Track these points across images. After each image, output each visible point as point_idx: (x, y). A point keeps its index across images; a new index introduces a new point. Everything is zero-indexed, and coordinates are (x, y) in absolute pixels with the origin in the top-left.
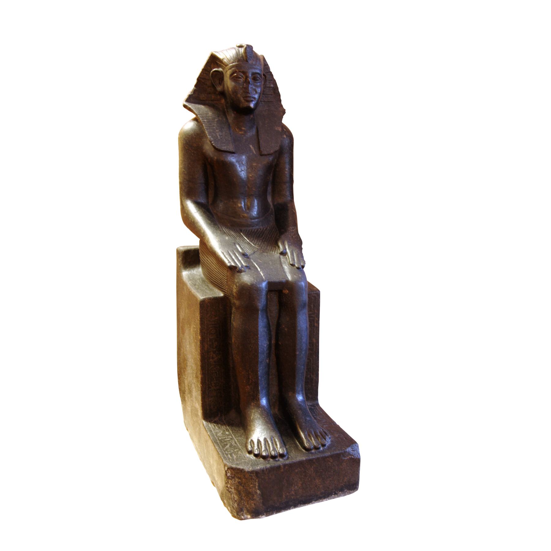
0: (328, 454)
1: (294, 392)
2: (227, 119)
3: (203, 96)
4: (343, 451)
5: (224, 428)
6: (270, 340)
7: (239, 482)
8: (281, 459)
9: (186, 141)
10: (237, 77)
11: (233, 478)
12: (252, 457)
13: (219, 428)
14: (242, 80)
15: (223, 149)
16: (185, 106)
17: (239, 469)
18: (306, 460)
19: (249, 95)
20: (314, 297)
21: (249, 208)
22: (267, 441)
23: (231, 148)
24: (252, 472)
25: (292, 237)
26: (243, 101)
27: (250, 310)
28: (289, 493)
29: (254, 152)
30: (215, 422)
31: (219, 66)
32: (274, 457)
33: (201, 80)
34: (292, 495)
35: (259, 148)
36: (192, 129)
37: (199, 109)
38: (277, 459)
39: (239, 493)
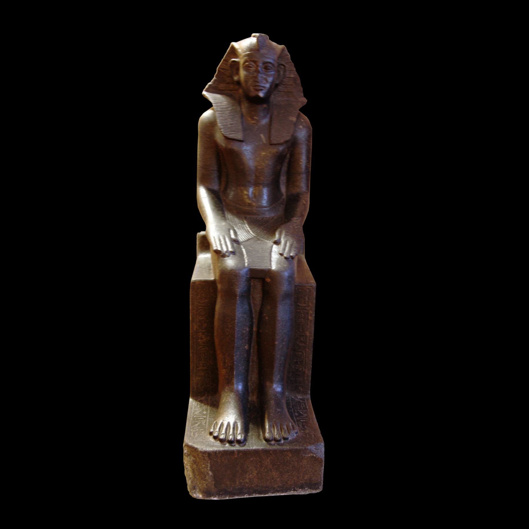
0: (287, 447)
1: (272, 382)
2: (241, 108)
3: (222, 86)
4: (303, 448)
5: (205, 407)
6: (251, 327)
7: (193, 460)
8: (237, 445)
11: (189, 455)
12: (211, 439)
13: (201, 407)
17: (193, 448)
18: (262, 450)
20: (309, 289)
21: (258, 196)
22: (237, 425)
23: (239, 136)
24: (205, 452)
25: (294, 227)
27: (230, 294)
28: (243, 480)
30: (201, 401)
32: (231, 442)
33: (222, 71)
34: (247, 483)
35: (270, 137)
37: (215, 99)
38: (233, 445)
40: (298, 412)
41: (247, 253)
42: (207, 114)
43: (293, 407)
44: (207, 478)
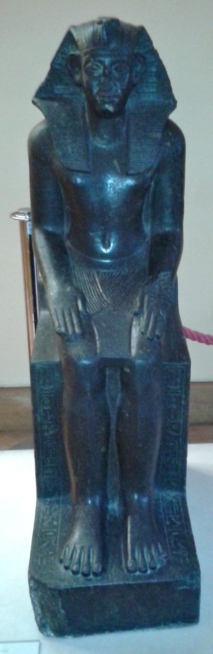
7: (41, 596)
16: (34, 103)
39: (42, 608)
40: (170, 519)
41: (98, 333)
43: (164, 511)
44: (59, 616)
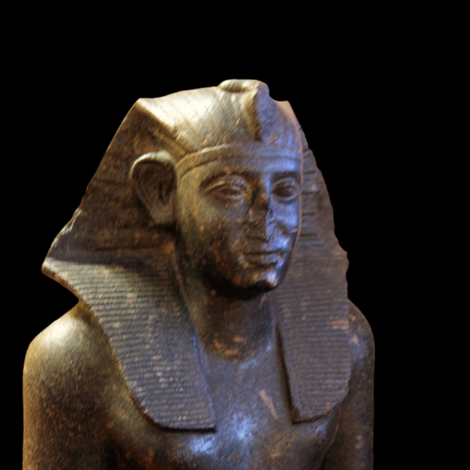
2: (185, 310)
3: (105, 235)
9: (49, 391)
10: (227, 190)
14: (241, 199)
15: (176, 425)
19: (264, 247)
26: (246, 265)
29: (273, 412)
31: (158, 145)
36: (69, 352)
42: (59, 334)
